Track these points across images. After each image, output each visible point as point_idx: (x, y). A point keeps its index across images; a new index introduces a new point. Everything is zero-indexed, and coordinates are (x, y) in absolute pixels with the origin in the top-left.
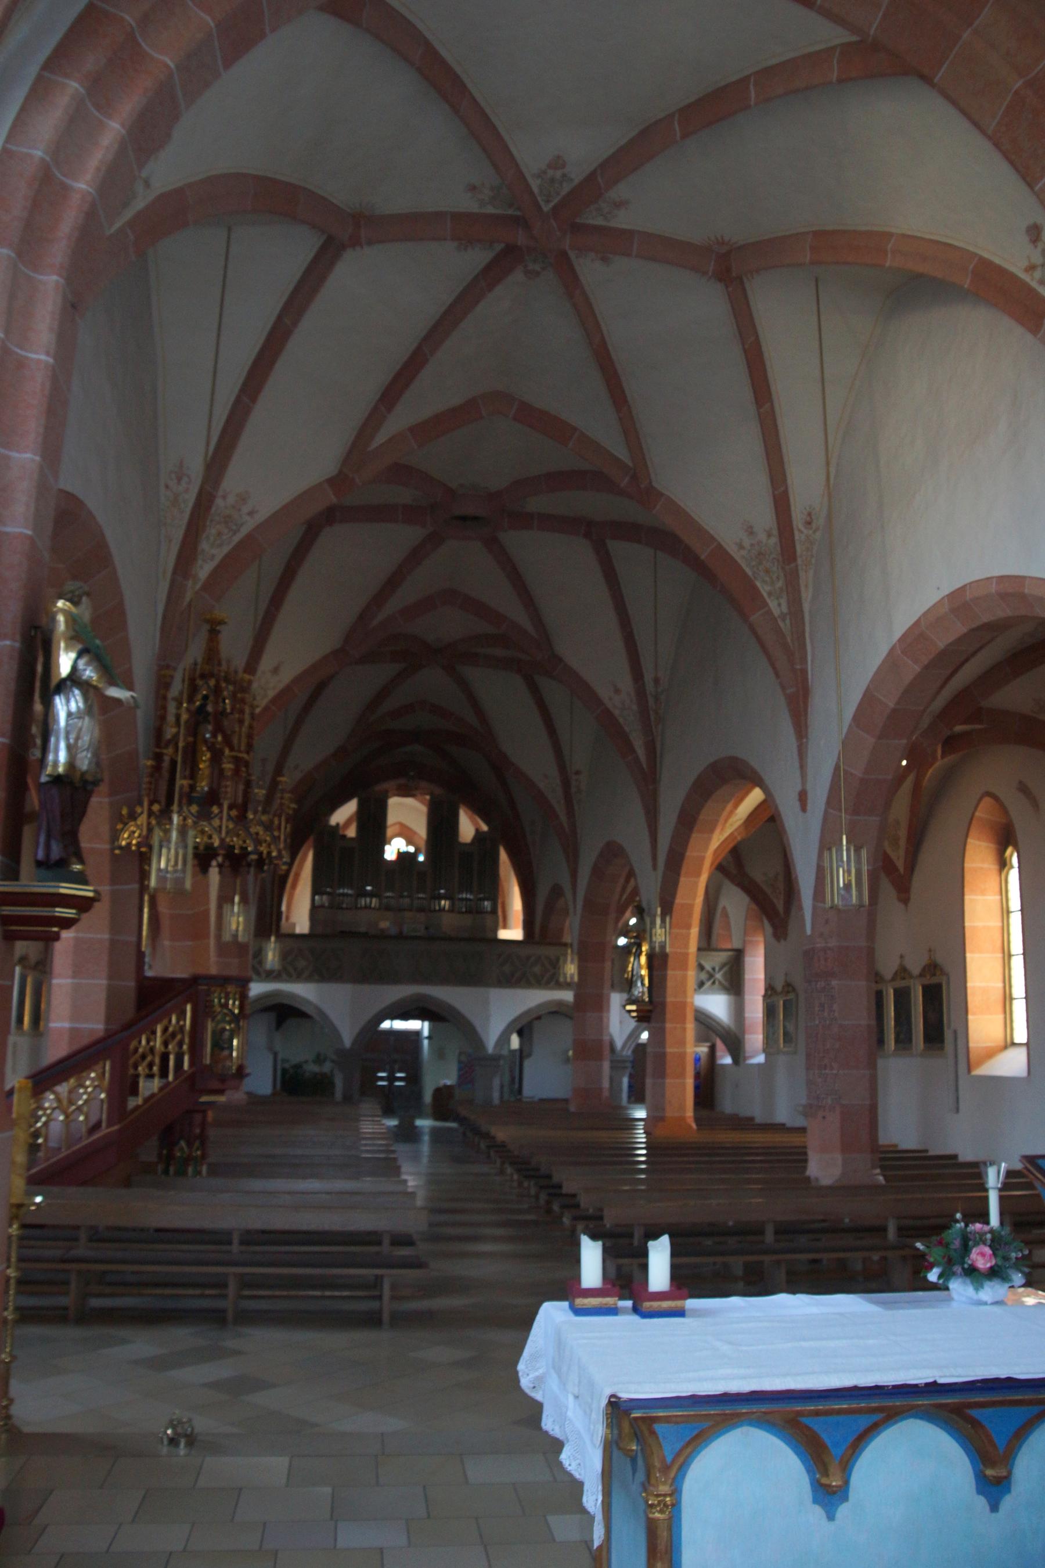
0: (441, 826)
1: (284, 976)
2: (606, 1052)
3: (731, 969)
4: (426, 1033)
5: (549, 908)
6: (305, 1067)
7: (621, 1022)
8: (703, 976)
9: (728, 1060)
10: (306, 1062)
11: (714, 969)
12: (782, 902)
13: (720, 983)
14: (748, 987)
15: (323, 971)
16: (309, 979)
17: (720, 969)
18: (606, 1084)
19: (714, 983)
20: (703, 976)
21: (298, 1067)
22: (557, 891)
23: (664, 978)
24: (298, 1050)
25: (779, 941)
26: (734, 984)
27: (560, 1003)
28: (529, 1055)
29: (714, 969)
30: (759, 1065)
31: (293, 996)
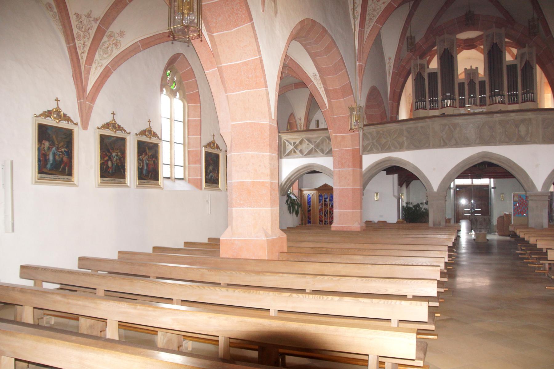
1: (392, 148)
6: (421, 206)
10: (422, 203)
15: (419, 143)
16: (408, 148)
21: (418, 205)
31: (399, 160)
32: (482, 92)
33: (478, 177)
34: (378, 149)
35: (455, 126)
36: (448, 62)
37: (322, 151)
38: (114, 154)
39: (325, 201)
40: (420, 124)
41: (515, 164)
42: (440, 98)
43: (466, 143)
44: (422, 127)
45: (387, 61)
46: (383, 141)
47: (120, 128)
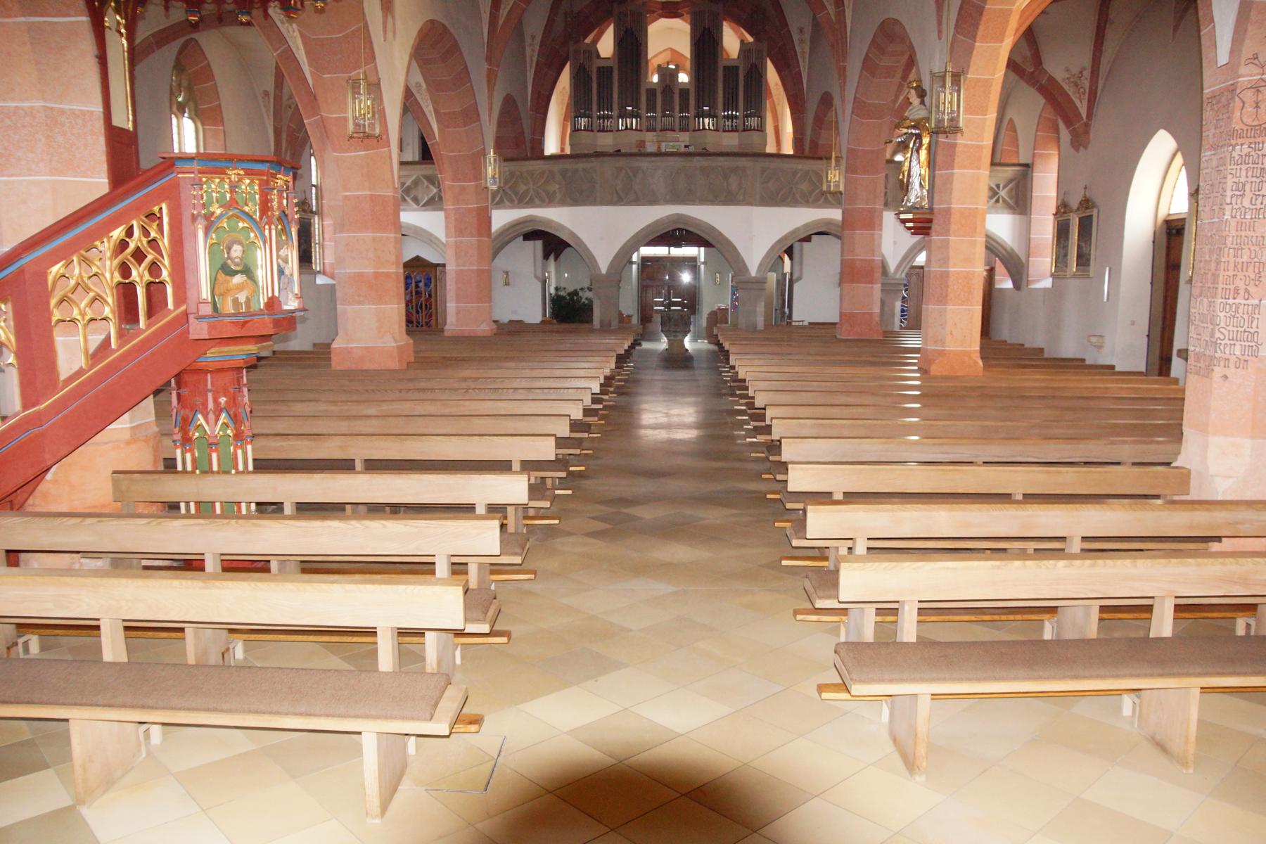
0: (705, 44)
1: (537, 201)
2: (878, 274)
3: (1017, 185)
4: (702, 259)
5: (820, 121)
7: (895, 243)
9: (1008, 284)
11: (998, 186)
12: (1085, 103)
13: (1004, 200)
14: (1036, 204)
15: (579, 195)
16: (563, 203)
17: (1005, 187)
18: (876, 310)
19: (997, 201)
21: (575, 293)
22: (826, 101)
23: (949, 180)
24: (559, 277)
25: (1077, 150)
26: (1018, 198)
27: (829, 222)
28: (799, 279)
29: (998, 186)
30: (1045, 290)
31: (549, 222)
32: (685, 108)
33: (678, 245)
34: (512, 201)
35: (635, 171)
36: (631, 45)
37: (416, 200)
39: (417, 286)
40: (582, 165)
41: (721, 234)
42: (615, 113)
43: (652, 200)
44: (584, 170)
45: (528, 40)
46: (522, 188)
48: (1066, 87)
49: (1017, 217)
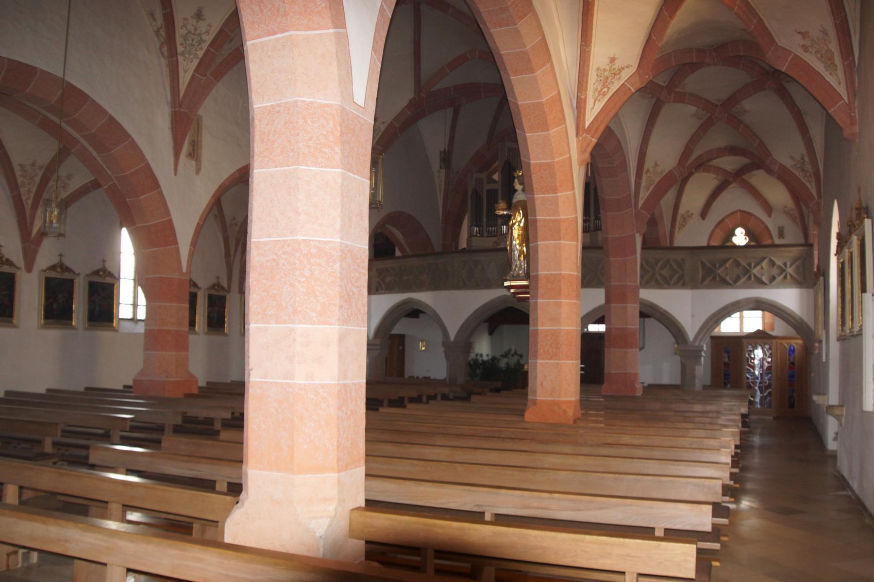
7: (693, 316)
8: (775, 271)
11: (785, 264)
12: (813, 184)
17: (791, 265)
20: (775, 271)
38: (60, 296)
47: (67, 269)
48: (796, 172)
49: (804, 290)
